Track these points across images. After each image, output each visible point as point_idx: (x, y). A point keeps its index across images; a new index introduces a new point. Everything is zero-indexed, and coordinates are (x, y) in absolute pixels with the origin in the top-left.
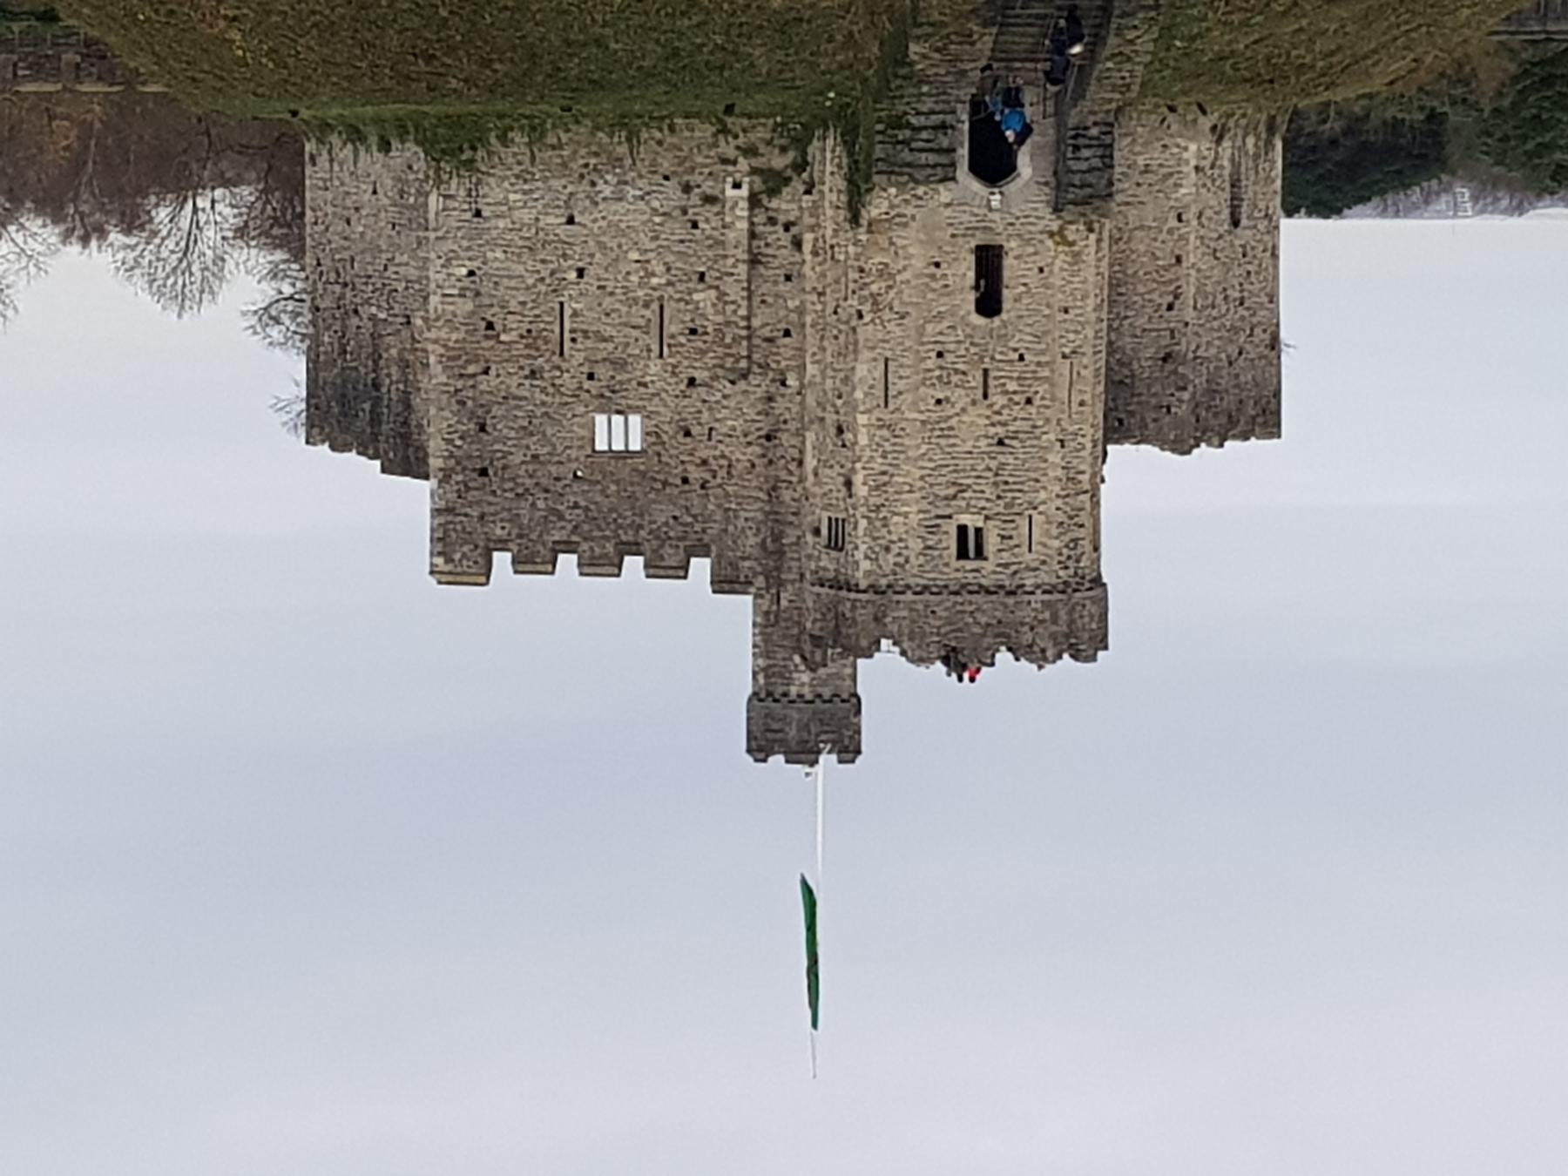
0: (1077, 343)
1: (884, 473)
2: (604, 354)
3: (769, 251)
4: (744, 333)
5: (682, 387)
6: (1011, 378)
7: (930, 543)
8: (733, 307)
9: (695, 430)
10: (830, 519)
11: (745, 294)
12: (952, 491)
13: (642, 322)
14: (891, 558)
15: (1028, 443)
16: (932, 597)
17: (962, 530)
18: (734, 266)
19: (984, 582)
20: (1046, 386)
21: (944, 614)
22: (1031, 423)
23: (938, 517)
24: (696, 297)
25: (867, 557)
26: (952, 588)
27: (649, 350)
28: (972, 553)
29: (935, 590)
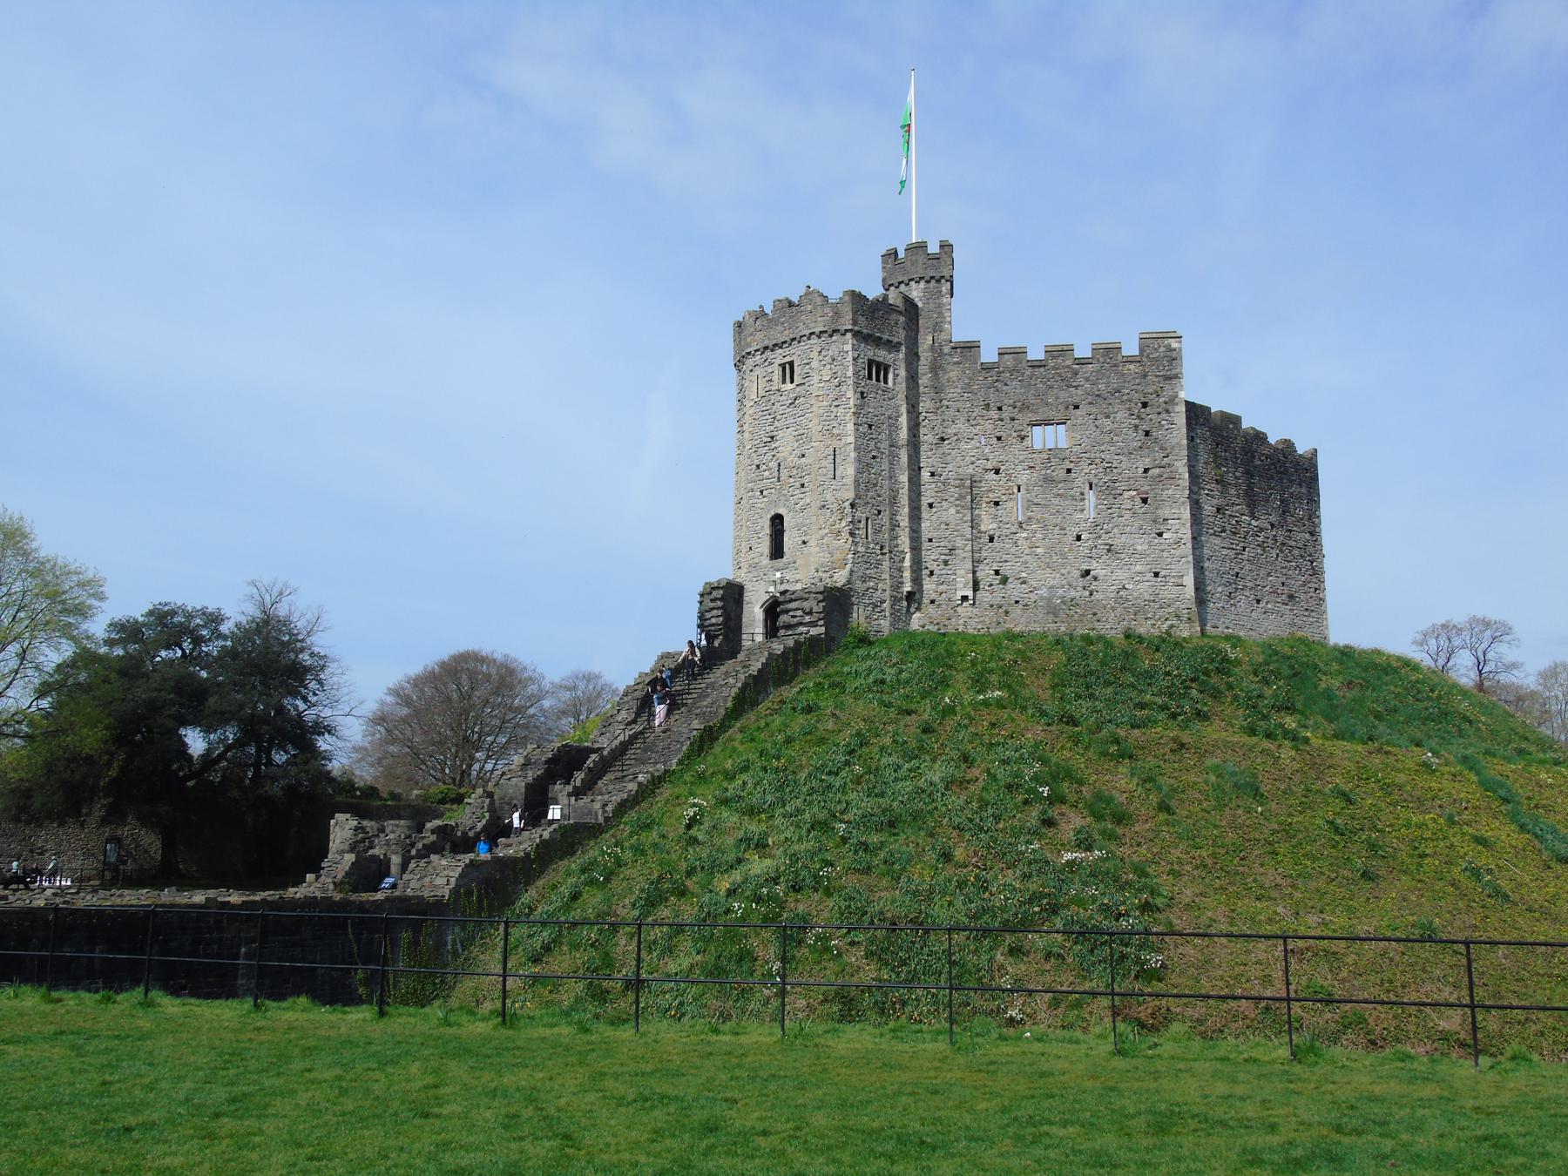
2: (1060, 486)
3: (943, 557)
7: (807, 367)
8: (965, 519)
10: (886, 382)
14: (830, 353)
17: (792, 382)
19: (780, 351)
28: (787, 366)
29: (804, 338)
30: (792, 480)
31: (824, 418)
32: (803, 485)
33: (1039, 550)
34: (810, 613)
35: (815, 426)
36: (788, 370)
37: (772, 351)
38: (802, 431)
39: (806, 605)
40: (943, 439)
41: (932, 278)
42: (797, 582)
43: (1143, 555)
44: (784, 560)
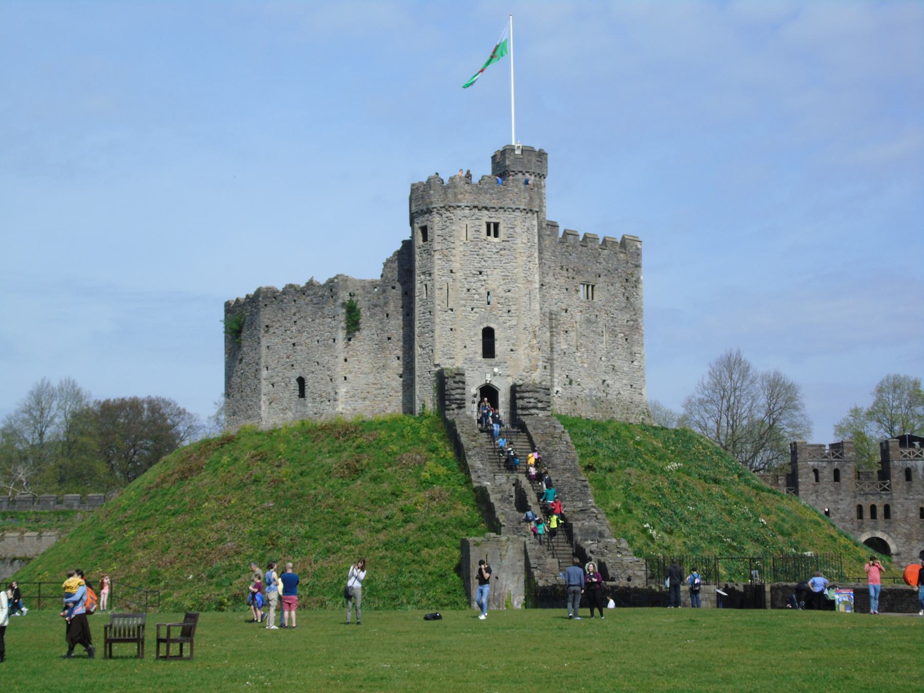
0: (444, 316)
1: (530, 262)
2: (594, 325)
4: (554, 330)
5: (569, 309)
6: (477, 300)
7: (511, 230)
9: (565, 291)
11: (555, 346)
12: (502, 252)
13: (583, 338)
15: (468, 272)
16: (511, 206)
17: (496, 235)
18: (558, 358)
19: (486, 212)
20: (461, 296)
21: (505, 199)
22: (467, 281)
23: (508, 241)
24: (566, 347)
25: (534, 226)
26: (502, 210)
27: (580, 326)
29: (510, 210)
30: (499, 306)
31: (524, 268)
32: (509, 311)
33: (586, 365)
34: (541, 402)
35: (520, 273)
36: (493, 229)
37: (479, 210)
38: (507, 274)
39: (540, 396)
40: (542, 285)
41: (539, 174)
42: (508, 376)
43: (627, 374)
44: (496, 359)
